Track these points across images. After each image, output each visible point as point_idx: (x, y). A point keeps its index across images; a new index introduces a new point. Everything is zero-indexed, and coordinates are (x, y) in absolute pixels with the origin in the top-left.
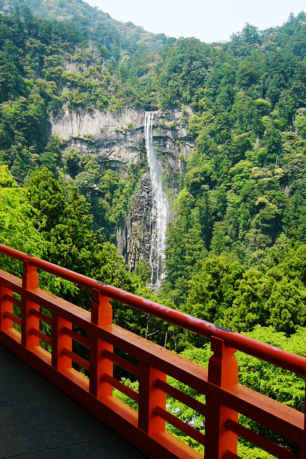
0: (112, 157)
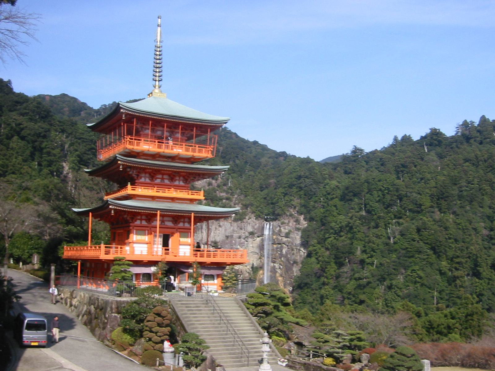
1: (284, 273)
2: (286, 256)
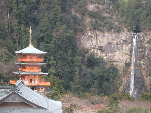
0: (113, 59)
1: (146, 68)
2: (148, 57)
